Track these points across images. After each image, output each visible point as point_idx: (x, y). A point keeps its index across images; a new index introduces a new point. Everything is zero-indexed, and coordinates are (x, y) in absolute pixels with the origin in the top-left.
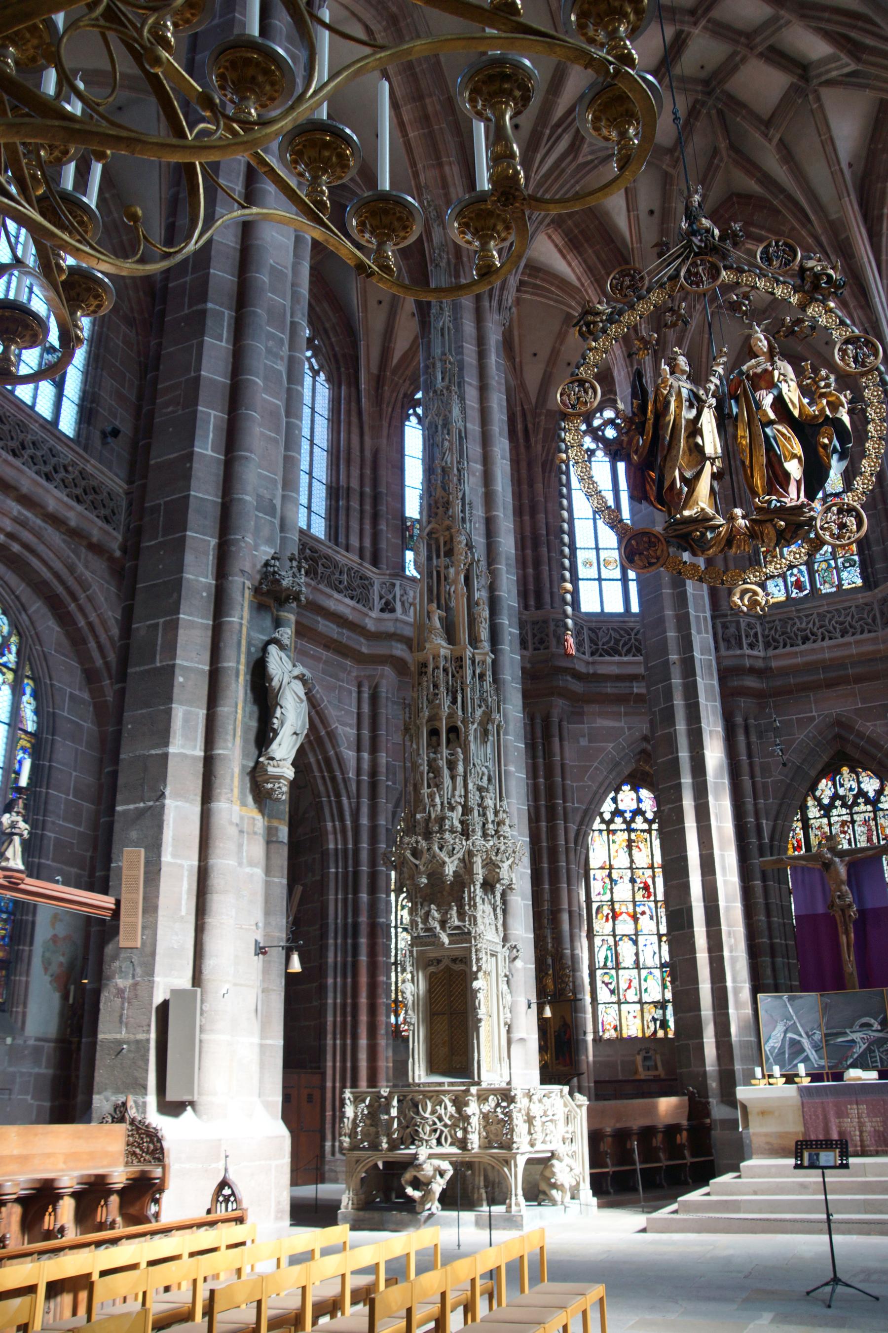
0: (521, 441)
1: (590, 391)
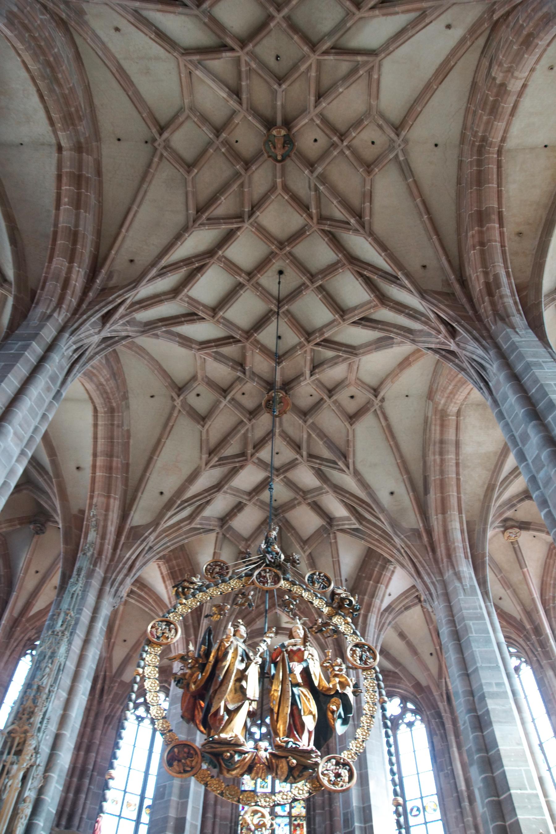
0: (97, 696)
1: (173, 631)
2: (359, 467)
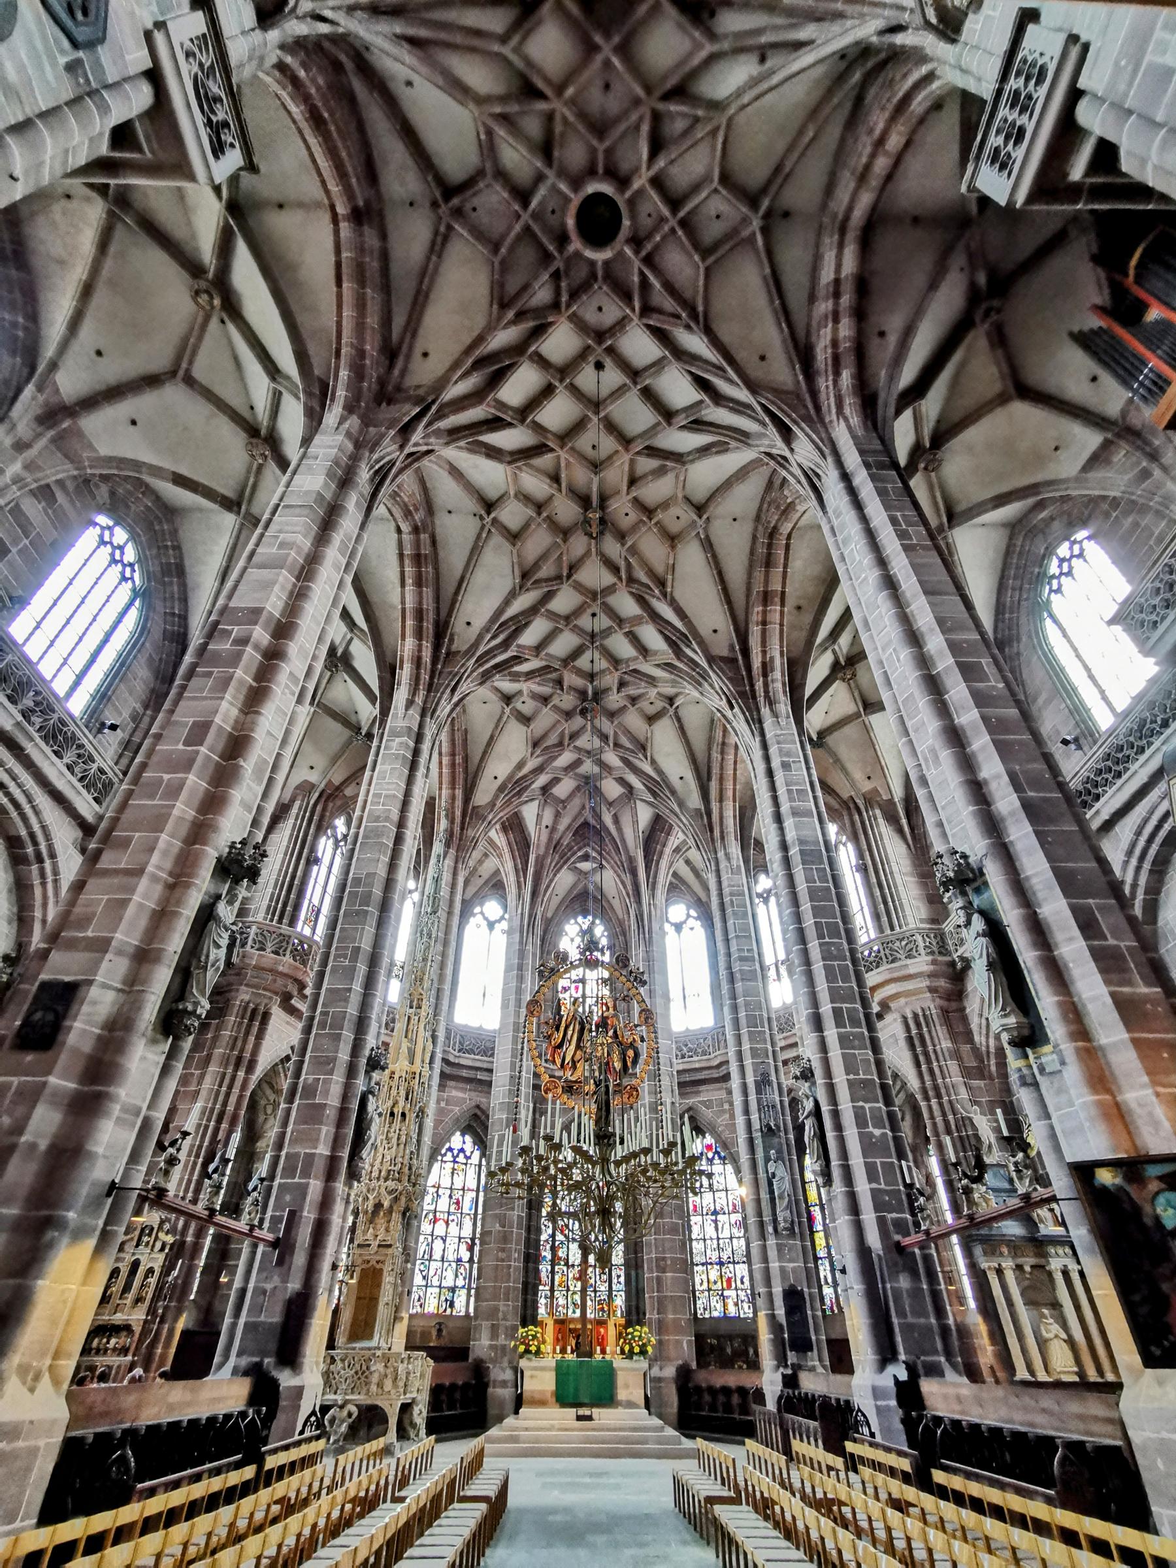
2: (656, 757)
